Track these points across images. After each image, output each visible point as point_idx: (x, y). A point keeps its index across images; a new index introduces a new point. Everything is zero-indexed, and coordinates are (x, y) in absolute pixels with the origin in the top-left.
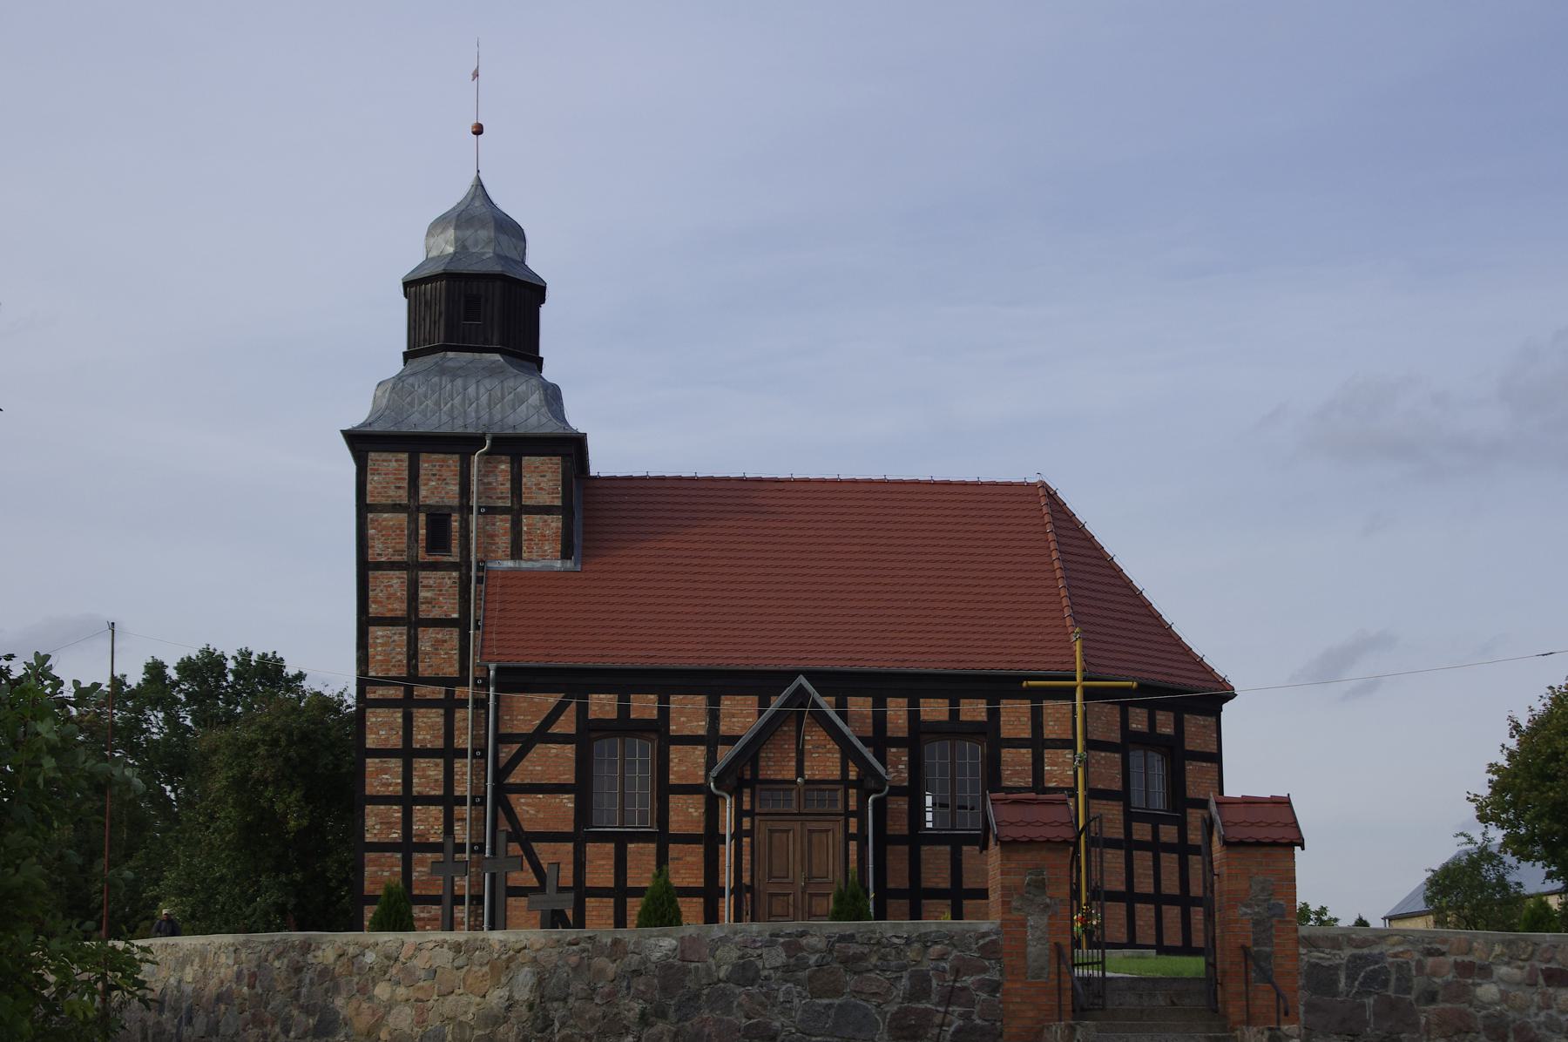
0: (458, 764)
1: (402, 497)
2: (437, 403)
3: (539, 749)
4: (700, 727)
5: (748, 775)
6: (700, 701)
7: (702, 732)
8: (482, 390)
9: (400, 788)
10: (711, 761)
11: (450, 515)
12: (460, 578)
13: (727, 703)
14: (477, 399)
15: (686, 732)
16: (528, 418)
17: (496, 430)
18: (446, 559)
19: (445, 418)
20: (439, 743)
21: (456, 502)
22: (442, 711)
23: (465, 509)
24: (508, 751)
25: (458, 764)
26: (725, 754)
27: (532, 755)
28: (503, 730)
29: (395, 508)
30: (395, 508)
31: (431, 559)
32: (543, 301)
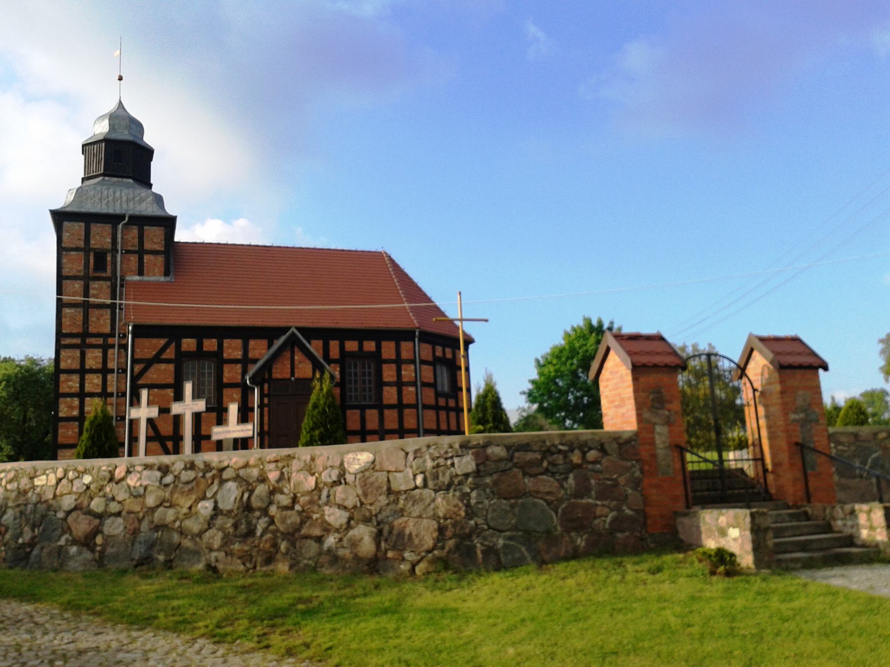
0: (109, 377)
1: (82, 244)
2: (100, 200)
3: (156, 366)
4: (238, 354)
5: (267, 377)
6: (239, 342)
7: (239, 357)
8: (123, 194)
9: (78, 389)
10: (244, 372)
11: (106, 253)
12: (112, 284)
13: (252, 343)
14: (121, 198)
15: (232, 357)
16: (147, 209)
17: (131, 212)
18: (104, 275)
19: (104, 207)
20: (100, 366)
21: (110, 247)
22: (101, 350)
23: (114, 250)
24: (138, 368)
25: (109, 377)
26: (253, 369)
27: (152, 369)
28: (136, 357)
29: (77, 249)
30: (77, 249)
31: (97, 275)
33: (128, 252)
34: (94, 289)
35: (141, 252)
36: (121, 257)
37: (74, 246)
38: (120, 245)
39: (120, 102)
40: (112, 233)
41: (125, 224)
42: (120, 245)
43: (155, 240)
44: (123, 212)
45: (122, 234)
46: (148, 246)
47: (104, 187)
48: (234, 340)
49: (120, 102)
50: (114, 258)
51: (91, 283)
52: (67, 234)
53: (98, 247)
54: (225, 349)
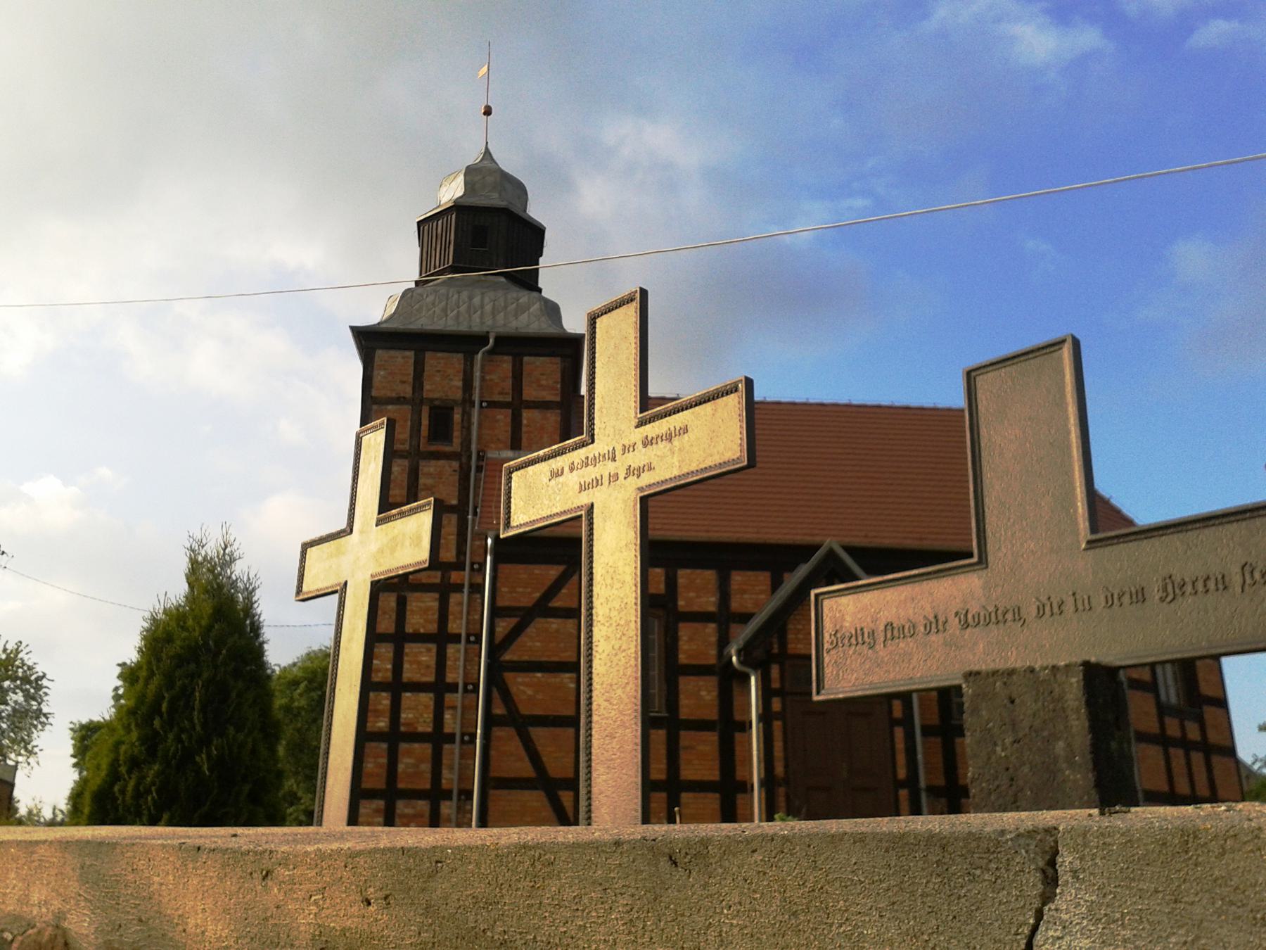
0: (451, 650)
1: (407, 391)
2: (445, 310)
3: (540, 623)
4: (709, 602)
6: (710, 575)
7: (712, 608)
8: (487, 300)
9: (389, 675)
10: (723, 642)
11: (452, 409)
12: (461, 467)
13: (737, 578)
14: (482, 307)
15: (696, 608)
16: (530, 323)
17: (501, 330)
18: (447, 449)
19: (450, 322)
20: (433, 628)
21: (459, 395)
22: (437, 595)
23: (467, 402)
25: (451, 650)
27: (531, 630)
28: (501, 603)
29: (399, 400)
30: (399, 400)
31: (433, 448)
32: (541, 256)
33: (493, 405)
34: (429, 475)
35: (517, 405)
36: (480, 414)
37: (394, 395)
38: (477, 391)
39: (487, 150)
40: (465, 372)
41: (491, 352)
42: (477, 391)
43: (544, 382)
44: (485, 329)
45: (483, 367)
46: (529, 393)
47: (452, 290)
48: (699, 571)
49: (487, 150)
50: (467, 416)
51: (422, 463)
52: (382, 373)
53: (436, 395)
54: (680, 590)
